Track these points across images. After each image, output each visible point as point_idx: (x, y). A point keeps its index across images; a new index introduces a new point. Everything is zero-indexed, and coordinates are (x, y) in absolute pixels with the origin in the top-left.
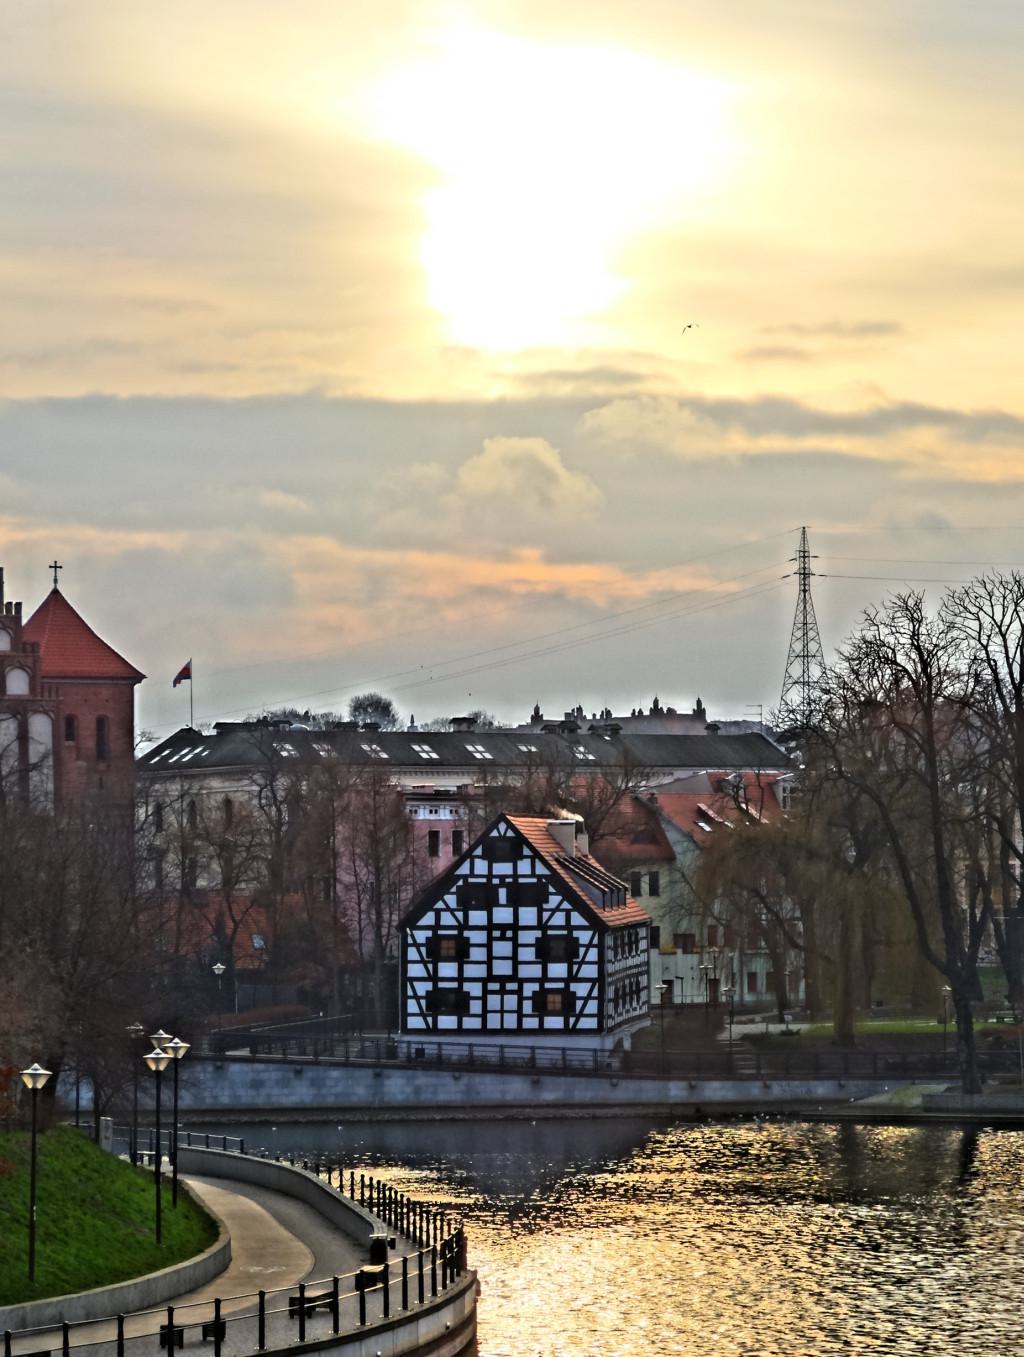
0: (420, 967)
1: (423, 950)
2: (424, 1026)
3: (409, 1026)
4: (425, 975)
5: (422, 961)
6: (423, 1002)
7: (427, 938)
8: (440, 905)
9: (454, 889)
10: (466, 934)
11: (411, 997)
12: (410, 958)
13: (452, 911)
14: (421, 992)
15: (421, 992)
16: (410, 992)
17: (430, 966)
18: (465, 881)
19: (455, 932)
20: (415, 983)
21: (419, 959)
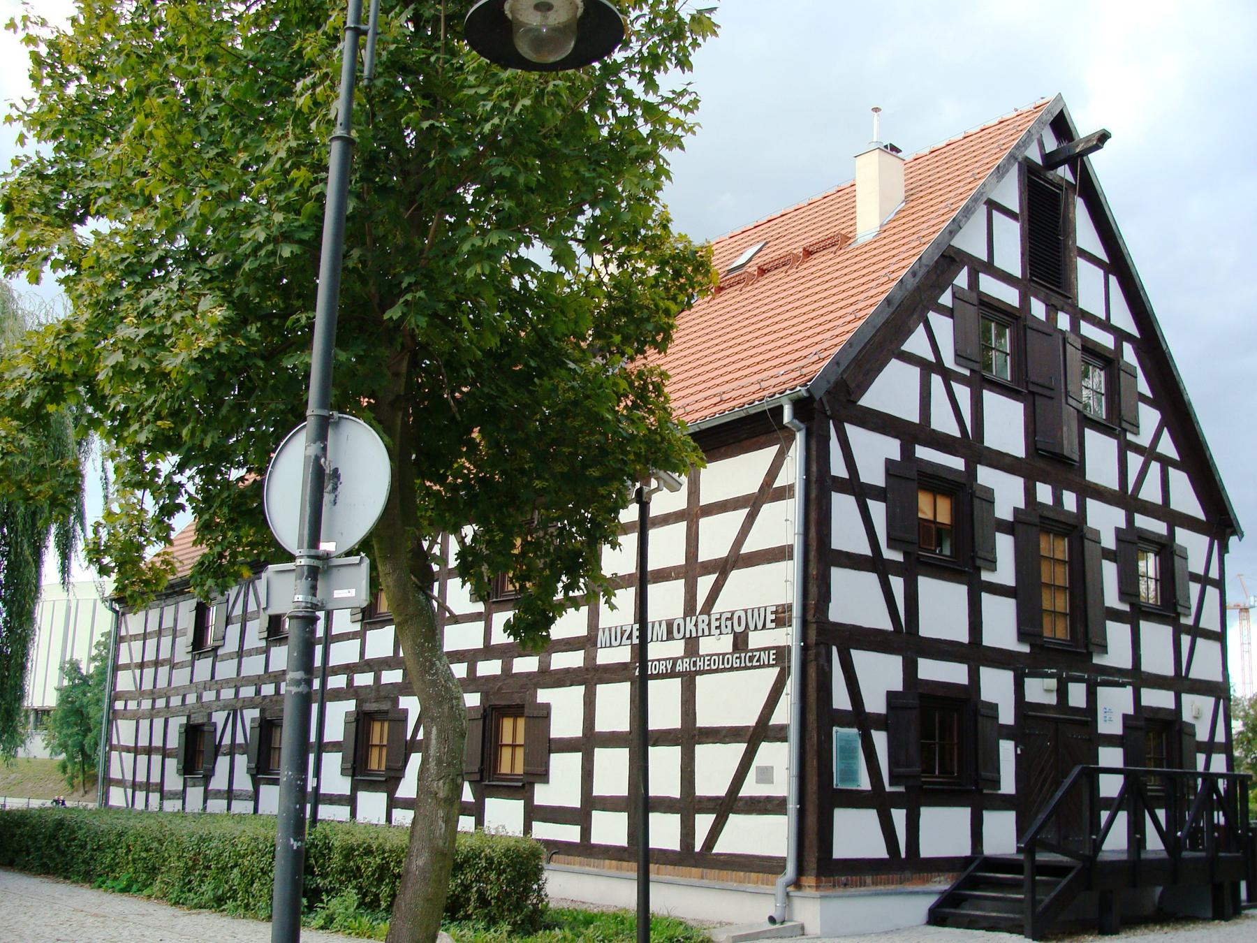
0: (871, 579)
1: (878, 510)
2: (881, 852)
3: (842, 849)
4: (887, 625)
5: (873, 563)
6: (880, 739)
7: (889, 463)
8: (917, 343)
9: (946, 299)
10: (986, 476)
11: (843, 719)
12: (838, 543)
13: (948, 376)
14: (875, 704)
15: (875, 704)
16: (841, 700)
17: (897, 584)
18: (973, 282)
19: (958, 463)
20: (860, 658)
21: (866, 550)
